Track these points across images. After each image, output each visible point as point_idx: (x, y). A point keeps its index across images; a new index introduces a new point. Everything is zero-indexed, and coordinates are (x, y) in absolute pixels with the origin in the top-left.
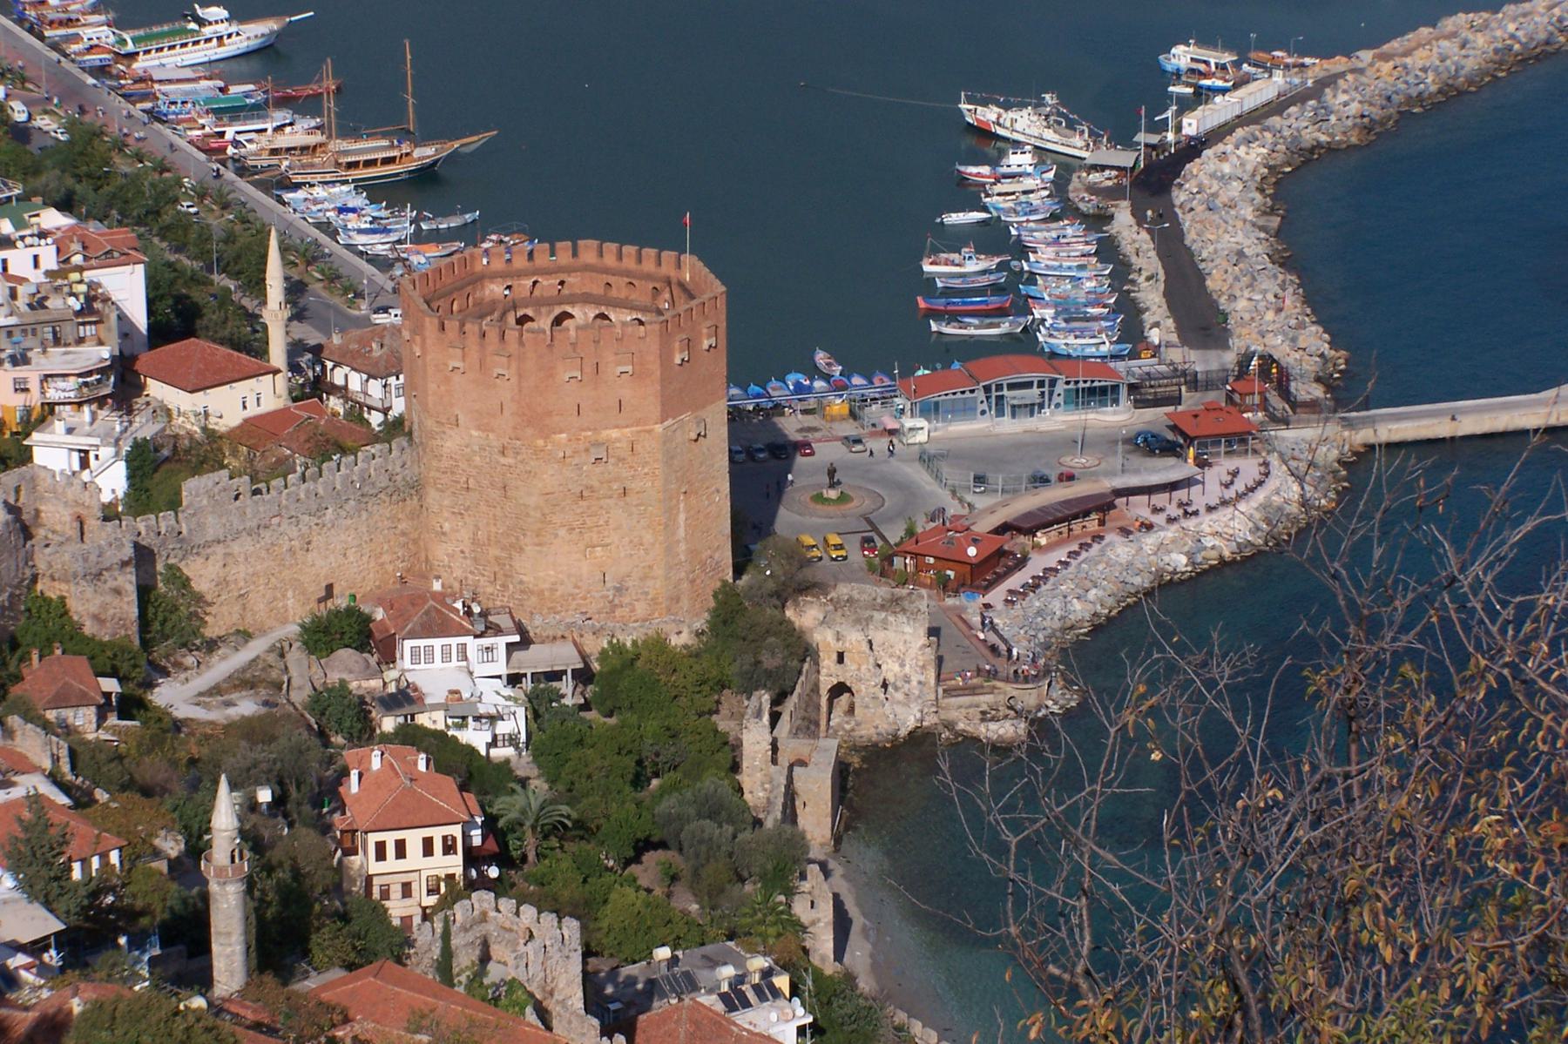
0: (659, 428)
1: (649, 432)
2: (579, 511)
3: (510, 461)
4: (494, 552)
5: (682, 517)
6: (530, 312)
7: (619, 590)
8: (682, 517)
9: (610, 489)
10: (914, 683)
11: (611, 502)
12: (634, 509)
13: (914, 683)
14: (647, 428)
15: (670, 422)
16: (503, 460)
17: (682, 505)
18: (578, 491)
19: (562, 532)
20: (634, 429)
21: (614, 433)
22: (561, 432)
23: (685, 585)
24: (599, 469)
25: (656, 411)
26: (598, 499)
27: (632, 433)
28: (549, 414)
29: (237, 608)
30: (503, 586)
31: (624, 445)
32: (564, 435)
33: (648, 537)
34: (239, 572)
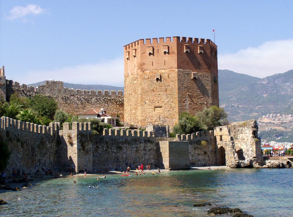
2: (153, 95)
9: (162, 89)
10: (250, 151)
11: (162, 93)
12: (169, 96)
14: (173, 70)
15: (181, 70)
18: (152, 89)
20: (169, 70)
21: (163, 71)
22: (147, 70)
25: (176, 66)
26: (158, 92)
27: (168, 71)
28: (144, 64)
32: (148, 71)
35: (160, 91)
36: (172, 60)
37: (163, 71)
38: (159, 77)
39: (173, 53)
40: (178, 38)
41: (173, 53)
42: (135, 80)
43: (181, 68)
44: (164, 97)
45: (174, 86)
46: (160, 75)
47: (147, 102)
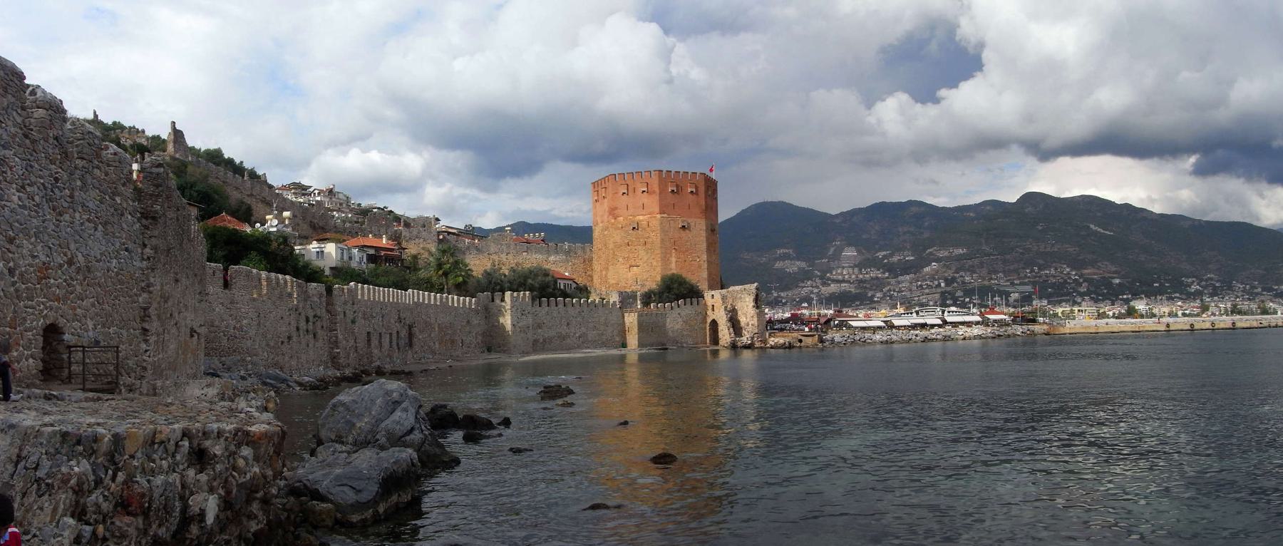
0: (659, 216)
1: (655, 217)
5: (674, 260)
10: (750, 325)
11: (640, 247)
13: (750, 325)
15: (665, 215)
17: (674, 255)
19: (621, 260)
21: (641, 218)
22: (621, 216)
24: (634, 232)
25: (657, 209)
28: (616, 208)
31: (645, 222)
33: (655, 264)
35: (637, 245)
36: (653, 203)
37: (641, 218)
38: (636, 226)
39: (654, 192)
40: (661, 171)
41: (654, 192)
42: (606, 230)
43: (664, 213)
44: (642, 253)
45: (655, 237)
46: (638, 223)
47: (621, 260)
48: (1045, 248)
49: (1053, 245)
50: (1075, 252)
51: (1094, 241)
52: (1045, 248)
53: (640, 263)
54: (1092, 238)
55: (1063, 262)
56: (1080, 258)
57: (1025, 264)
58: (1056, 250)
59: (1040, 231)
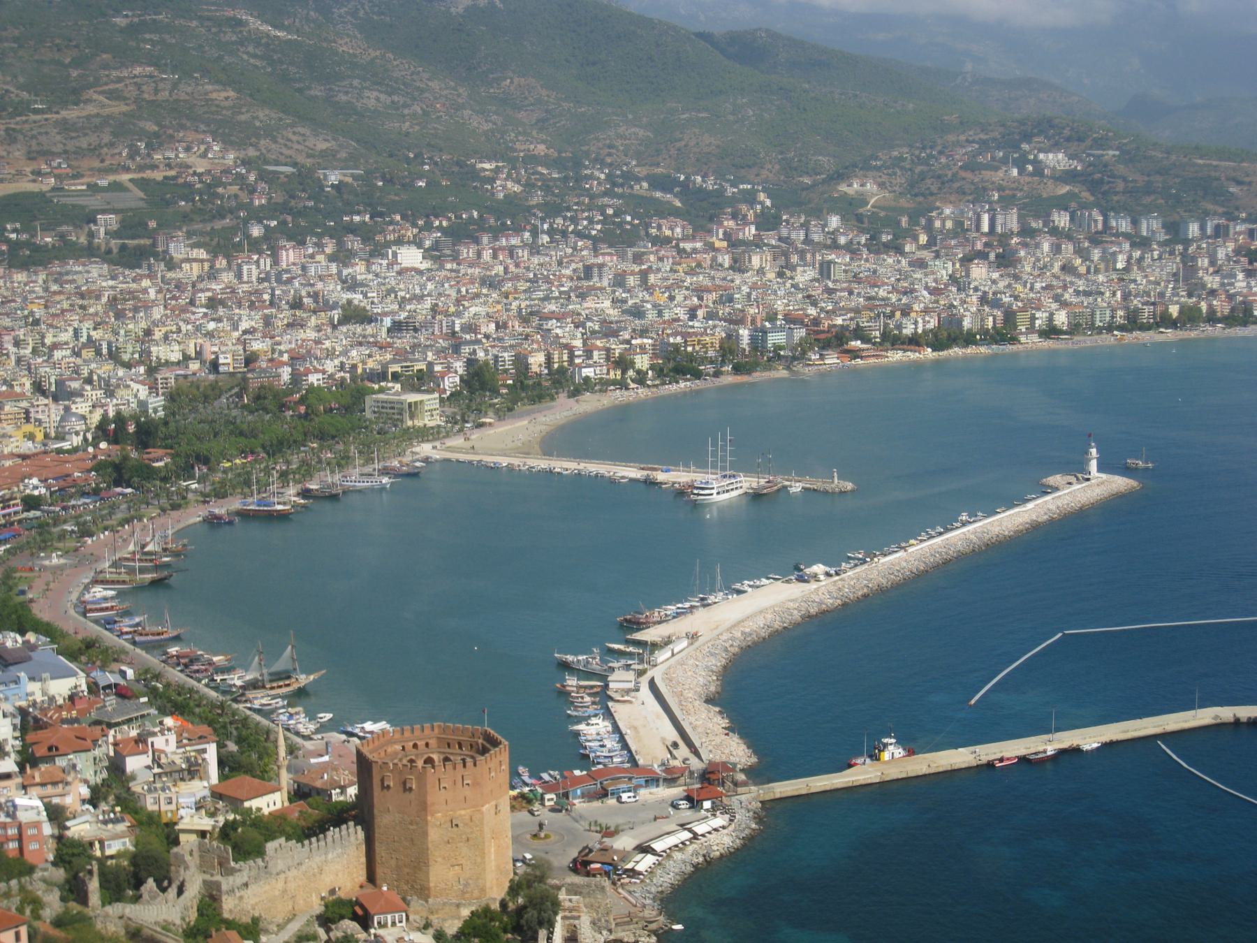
3: (415, 827)
4: (406, 870)
5: (493, 850)
6: (413, 757)
7: (466, 885)
8: (493, 850)
16: (411, 827)
18: (446, 839)
19: (439, 860)
21: (463, 812)
23: (495, 881)
29: (291, 903)
30: (412, 886)
34: (292, 886)
47: (439, 860)
48: (156, 91)
49: (175, 85)
50: (227, 104)
51: (255, 56)
52: (156, 91)
53: (463, 861)
54: (251, 49)
55: (203, 127)
56: (243, 118)
57: (114, 134)
58: (183, 97)
59: (122, 31)
